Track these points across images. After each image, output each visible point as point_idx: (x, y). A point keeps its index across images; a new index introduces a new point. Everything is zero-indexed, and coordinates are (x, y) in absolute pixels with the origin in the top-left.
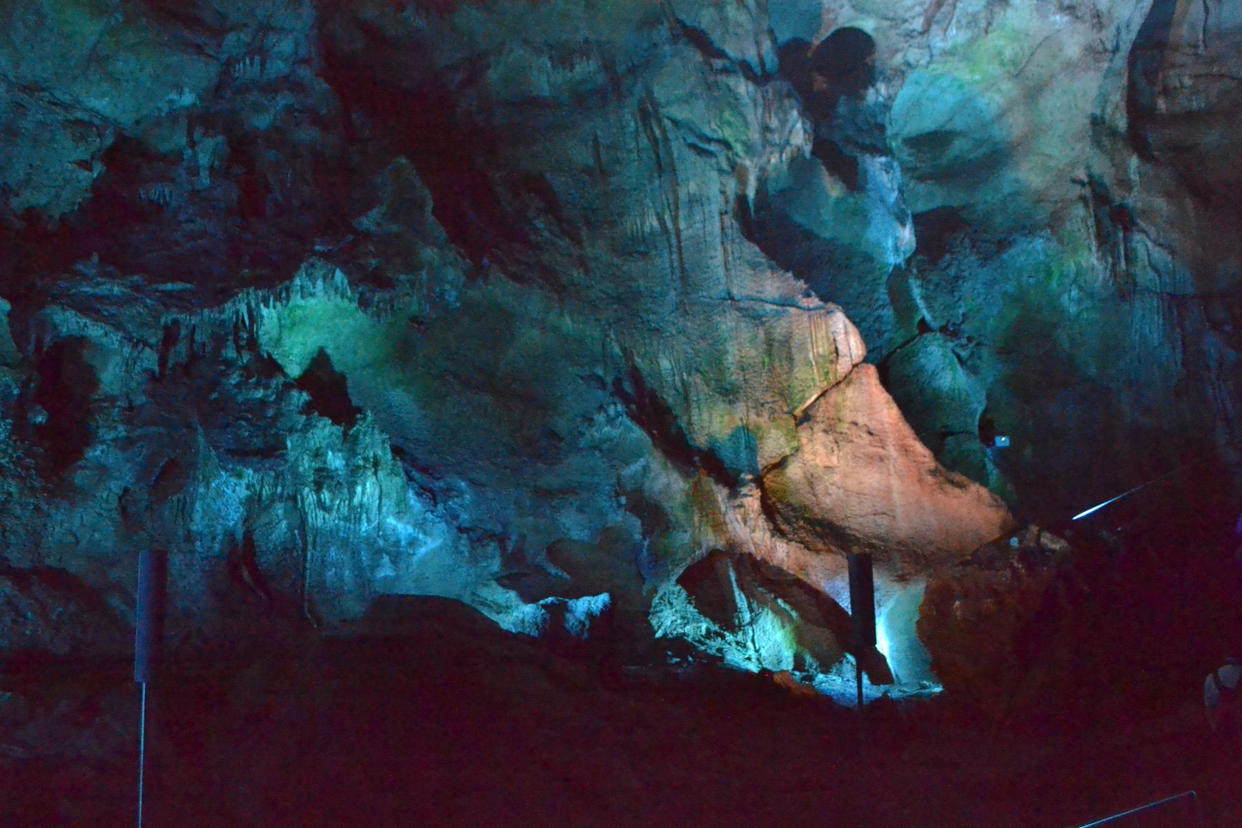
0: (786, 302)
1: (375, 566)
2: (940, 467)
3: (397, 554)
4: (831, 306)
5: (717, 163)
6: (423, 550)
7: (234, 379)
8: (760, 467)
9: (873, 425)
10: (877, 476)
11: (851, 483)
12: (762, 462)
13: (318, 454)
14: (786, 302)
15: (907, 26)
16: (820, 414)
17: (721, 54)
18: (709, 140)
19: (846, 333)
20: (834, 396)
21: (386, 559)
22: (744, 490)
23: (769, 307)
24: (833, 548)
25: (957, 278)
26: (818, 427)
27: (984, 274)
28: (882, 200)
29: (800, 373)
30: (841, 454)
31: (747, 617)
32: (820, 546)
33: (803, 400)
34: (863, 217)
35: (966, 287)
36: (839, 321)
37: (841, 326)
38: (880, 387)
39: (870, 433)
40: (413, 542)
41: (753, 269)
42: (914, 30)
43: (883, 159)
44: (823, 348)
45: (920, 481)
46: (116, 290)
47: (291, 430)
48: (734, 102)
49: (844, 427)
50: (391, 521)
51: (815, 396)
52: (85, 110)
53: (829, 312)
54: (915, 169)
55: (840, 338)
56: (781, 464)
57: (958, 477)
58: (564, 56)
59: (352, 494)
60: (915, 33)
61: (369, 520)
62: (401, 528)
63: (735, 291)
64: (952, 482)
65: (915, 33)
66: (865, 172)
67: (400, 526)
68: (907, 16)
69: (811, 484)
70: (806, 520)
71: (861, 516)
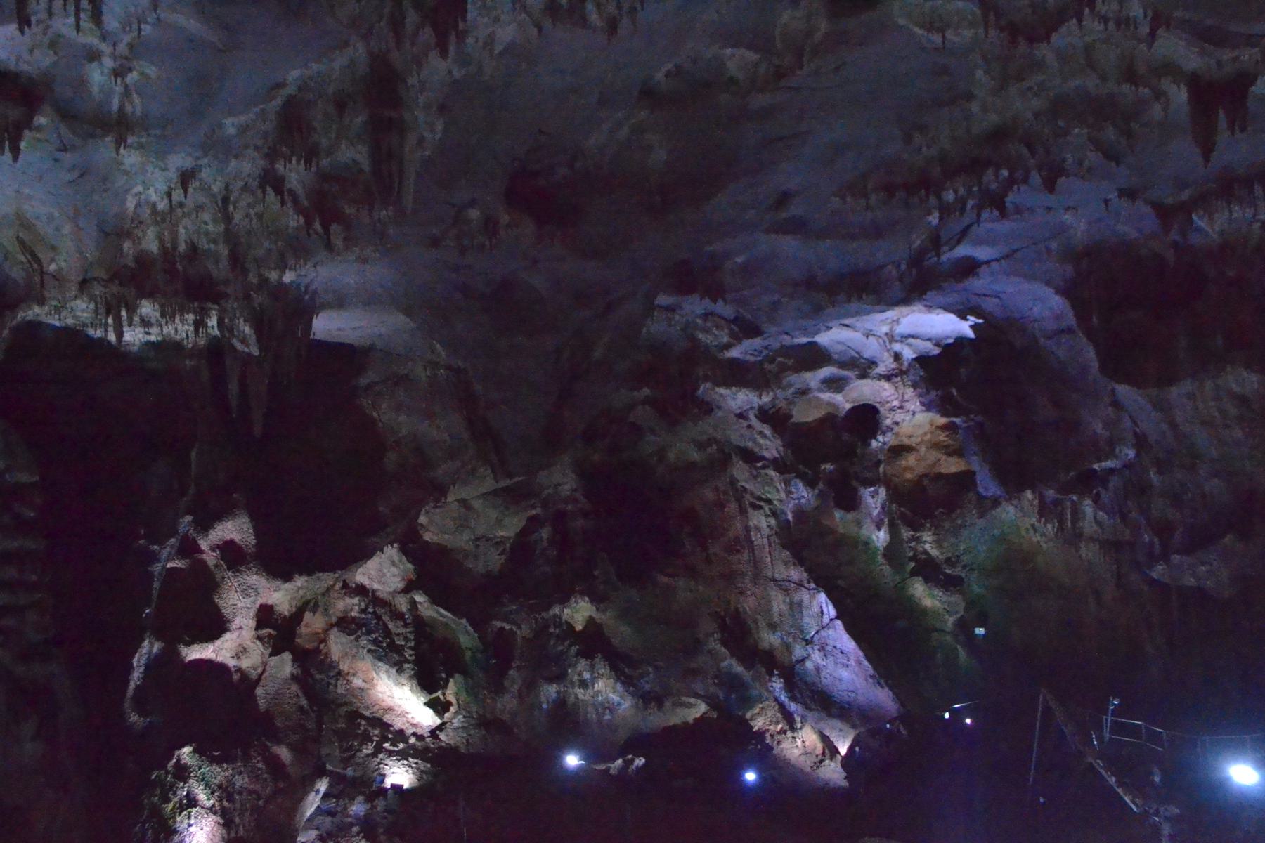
0: (800, 584)
1: (604, 714)
2: (876, 674)
3: (611, 708)
4: (821, 589)
5: (765, 512)
6: (623, 707)
7: (552, 642)
8: (794, 661)
9: (843, 648)
10: (846, 674)
11: (835, 675)
12: (794, 659)
13: (580, 674)
14: (800, 584)
15: (889, 405)
16: (815, 639)
17: (763, 458)
18: (760, 499)
19: (827, 603)
20: (823, 633)
21: (608, 711)
22: (774, 679)
23: (793, 585)
24: (819, 708)
25: (961, 526)
26: (816, 647)
27: (981, 523)
28: (870, 514)
29: (807, 620)
30: (828, 661)
31: (799, 725)
32: (813, 707)
33: (808, 633)
34: (859, 524)
35: (965, 533)
36: (822, 597)
37: (824, 599)
38: (845, 631)
39: (842, 653)
40: (619, 704)
41: (785, 565)
42: (894, 407)
43: (872, 489)
44: (816, 609)
45: (866, 680)
46: (514, 607)
47: (570, 666)
48: (770, 482)
49: (829, 648)
50: (611, 695)
51: (813, 633)
52: (498, 538)
53: (819, 592)
54: (947, 447)
55: (824, 606)
56: (802, 661)
57: (882, 681)
58: (701, 446)
59: (593, 688)
60: (895, 408)
61: (602, 696)
62: (614, 698)
63: (777, 576)
64: (879, 683)
65: (895, 408)
66: (861, 497)
67: (614, 697)
68: (889, 399)
69: (819, 673)
70: (812, 691)
71: (842, 691)
